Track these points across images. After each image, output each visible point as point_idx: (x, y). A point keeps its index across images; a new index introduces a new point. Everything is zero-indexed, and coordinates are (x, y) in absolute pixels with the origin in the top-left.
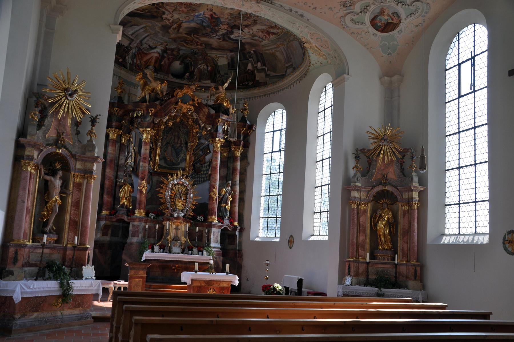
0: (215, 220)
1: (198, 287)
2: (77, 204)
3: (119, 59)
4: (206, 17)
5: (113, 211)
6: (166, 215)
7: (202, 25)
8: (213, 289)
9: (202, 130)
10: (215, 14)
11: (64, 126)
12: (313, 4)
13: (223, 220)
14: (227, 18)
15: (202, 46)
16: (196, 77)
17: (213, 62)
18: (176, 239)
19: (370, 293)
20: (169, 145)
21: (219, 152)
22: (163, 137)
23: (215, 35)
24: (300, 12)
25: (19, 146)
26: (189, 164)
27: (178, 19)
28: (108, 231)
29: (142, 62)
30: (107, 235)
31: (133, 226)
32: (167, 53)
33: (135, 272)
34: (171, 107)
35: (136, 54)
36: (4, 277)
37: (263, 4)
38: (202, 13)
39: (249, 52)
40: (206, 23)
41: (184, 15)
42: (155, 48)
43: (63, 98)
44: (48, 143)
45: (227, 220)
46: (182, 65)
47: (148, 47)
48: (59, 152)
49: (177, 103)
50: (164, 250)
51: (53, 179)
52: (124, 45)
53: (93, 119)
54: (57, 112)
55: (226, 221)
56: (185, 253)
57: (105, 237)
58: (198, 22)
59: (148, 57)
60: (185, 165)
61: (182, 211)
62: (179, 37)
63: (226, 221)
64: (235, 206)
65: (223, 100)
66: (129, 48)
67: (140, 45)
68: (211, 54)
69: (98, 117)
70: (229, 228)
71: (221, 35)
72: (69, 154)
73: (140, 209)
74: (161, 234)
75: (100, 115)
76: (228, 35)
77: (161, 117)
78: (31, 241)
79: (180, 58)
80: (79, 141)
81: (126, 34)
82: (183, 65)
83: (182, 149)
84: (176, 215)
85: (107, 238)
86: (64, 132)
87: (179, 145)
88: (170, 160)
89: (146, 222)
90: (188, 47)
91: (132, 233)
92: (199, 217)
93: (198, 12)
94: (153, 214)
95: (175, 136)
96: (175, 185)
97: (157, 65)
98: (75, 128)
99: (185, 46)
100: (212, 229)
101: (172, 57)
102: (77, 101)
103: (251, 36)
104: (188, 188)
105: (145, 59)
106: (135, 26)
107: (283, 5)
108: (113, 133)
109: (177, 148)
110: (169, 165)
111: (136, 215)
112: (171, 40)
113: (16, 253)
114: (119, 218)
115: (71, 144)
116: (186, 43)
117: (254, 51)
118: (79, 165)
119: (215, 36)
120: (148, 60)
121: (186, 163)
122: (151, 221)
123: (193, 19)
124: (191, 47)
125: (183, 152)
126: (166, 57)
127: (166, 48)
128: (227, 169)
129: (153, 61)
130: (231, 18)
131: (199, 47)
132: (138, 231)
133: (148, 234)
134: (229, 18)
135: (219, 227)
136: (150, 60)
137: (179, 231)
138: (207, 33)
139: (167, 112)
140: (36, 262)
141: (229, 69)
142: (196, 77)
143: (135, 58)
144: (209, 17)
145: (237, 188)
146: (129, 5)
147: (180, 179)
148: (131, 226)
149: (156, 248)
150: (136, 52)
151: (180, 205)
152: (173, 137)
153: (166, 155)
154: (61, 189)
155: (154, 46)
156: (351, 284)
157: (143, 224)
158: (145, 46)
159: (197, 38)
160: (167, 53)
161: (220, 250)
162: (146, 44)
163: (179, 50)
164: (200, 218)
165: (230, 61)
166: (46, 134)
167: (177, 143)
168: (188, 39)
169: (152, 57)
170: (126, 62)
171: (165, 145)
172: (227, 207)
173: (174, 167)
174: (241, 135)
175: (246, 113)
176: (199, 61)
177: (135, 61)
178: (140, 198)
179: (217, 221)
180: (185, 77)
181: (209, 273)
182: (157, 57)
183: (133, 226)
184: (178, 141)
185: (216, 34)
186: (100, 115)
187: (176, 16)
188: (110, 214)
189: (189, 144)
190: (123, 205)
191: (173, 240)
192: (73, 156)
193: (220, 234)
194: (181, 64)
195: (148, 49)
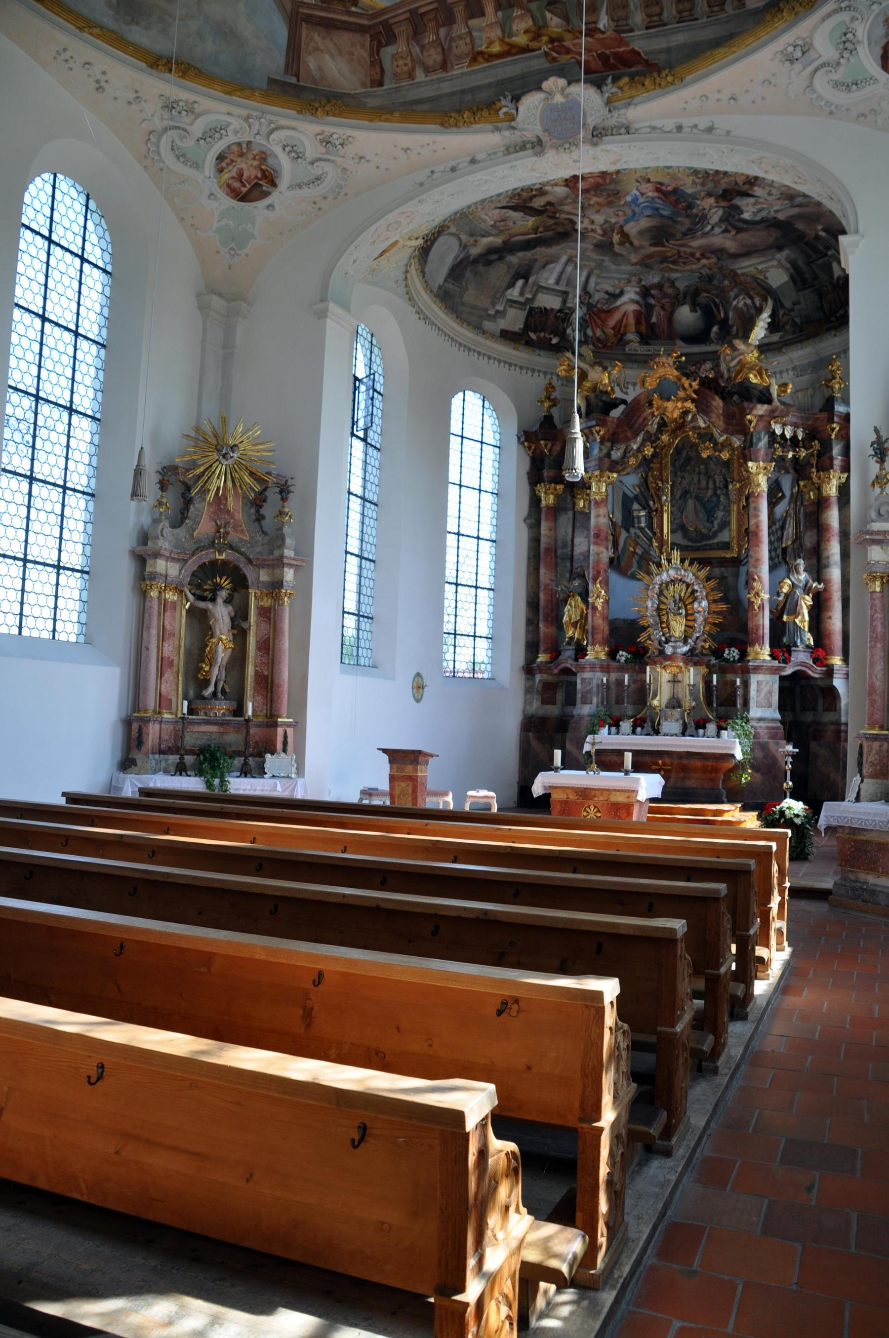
0: (763, 653)
1: (562, 802)
2: (268, 647)
3: (551, 339)
4: (653, 198)
5: (555, 653)
6: (650, 652)
7: (662, 216)
8: (595, 807)
9: (720, 451)
10: (661, 184)
12: (719, 91)
13: (790, 655)
14: (694, 182)
15: (708, 258)
16: (735, 329)
17: (758, 283)
18: (675, 703)
19: (882, 822)
20: (688, 496)
21: (765, 495)
22: (674, 482)
23: (709, 227)
24: (703, 123)
25: (141, 560)
26: (739, 531)
27: (606, 222)
28: (555, 694)
29: (605, 330)
30: (554, 703)
31: (583, 680)
32: (653, 297)
33: (398, 769)
34: (645, 414)
35: (587, 317)
37: (609, 143)
38: (635, 192)
39: (817, 237)
40: (664, 209)
41: (610, 211)
42: (622, 293)
45: (802, 653)
46: (696, 311)
47: (606, 297)
49: (651, 405)
50: (643, 728)
51: (210, 605)
52: (552, 309)
54: (205, 491)
55: (801, 658)
56: (687, 733)
57: (549, 707)
58: (649, 212)
59: (617, 316)
60: (730, 536)
61: (685, 642)
62: (651, 256)
63: (801, 658)
64: (830, 618)
65: (751, 369)
66: (567, 311)
67: (587, 298)
68: (743, 268)
69: (289, 483)
70: (810, 673)
71: (721, 220)
72: (242, 559)
73: (593, 644)
74: (642, 694)
76: (734, 217)
77: (627, 440)
79: (685, 298)
80: (263, 532)
81: (542, 284)
82: (699, 312)
83: (719, 501)
84: (669, 650)
85: (553, 710)
87: (710, 493)
88: (696, 528)
89: (606, 669)
90: (684, 271)
91: (582, 697)
92: (727, 652)
93: (627, 194)
94: (624, 653)
95: (699, 473)
96: (667, 584)
97: (643, 328)
98: (253, 511)
99: (676, 271)
100: (752, 676)
101: (667, 300)
103: (786, 199)
104: (696, 587)
105: (612, 322)
106: (552, 265)
107: (658, 123)
108: (546, 493)
109: (708, 501)
110: (690, 540)
111: (587, 658)
112: (638, 267)
114: (563, 666)
116: (673, 263)
117: (824, 230)
118: (264, 576)
119: (712, 228)
120: (618, 322)
121: (730, 530)
122: (622, 669)
123: (634, 214)
124: (688, 268)
125: (721, 507)
126: (655, 306)
127: (643, 286)
128: (818, 530)
129: (632, 320)
130: (702, 180)
131: (704, 261)
132: (590, 691)
133: (617, 697)
134: (698, 181)
135: (773, 671)
136: (624, 321)
137: (680, 684)
138: (690, 230)
139: (636, 426)
141: (799, 290)
142: (735, 329)
143: (587, 327)
144: (655, 194)
145: (835, 574)
147: (677, 569)
148: (579, 681)
149: (626, 725)
150: (585, 314)
151: (678, 627)
152: (696, 478)
153: (684, 520)
155: (617, 291)
156: (858, 799)
157: (599, 674)
158: (597, 297)
159: (683, 245)
160: (653, 297)
161: (779, 724)
162: (598, 291)
163: (672, 283)
164: (732, 653)
165: (792, 270)
167: (707, 488)
168: (669, 254)
169: (625, 313)
170: (570, 341)
171: (680, 498)
172: (797, 621)
173: (705, 543)
174: (834, 443)
175: (837, 386)
176: (728, 292)
177: (589, 332)
178: (593, 621)
179: (769, 658)
180: (713, 335)
181: (584, 773)
182: (634, 311)
183: (583, 680)
184: (708, 483)
185: (708, 223)
187: (599, 219)
188: (551, 662)
189: (730, 487)
190: (571, 638)
191: (667, 707)
192: (250, 561)
193: (777, 686)
194: (693, 310)
195: (607, 301)
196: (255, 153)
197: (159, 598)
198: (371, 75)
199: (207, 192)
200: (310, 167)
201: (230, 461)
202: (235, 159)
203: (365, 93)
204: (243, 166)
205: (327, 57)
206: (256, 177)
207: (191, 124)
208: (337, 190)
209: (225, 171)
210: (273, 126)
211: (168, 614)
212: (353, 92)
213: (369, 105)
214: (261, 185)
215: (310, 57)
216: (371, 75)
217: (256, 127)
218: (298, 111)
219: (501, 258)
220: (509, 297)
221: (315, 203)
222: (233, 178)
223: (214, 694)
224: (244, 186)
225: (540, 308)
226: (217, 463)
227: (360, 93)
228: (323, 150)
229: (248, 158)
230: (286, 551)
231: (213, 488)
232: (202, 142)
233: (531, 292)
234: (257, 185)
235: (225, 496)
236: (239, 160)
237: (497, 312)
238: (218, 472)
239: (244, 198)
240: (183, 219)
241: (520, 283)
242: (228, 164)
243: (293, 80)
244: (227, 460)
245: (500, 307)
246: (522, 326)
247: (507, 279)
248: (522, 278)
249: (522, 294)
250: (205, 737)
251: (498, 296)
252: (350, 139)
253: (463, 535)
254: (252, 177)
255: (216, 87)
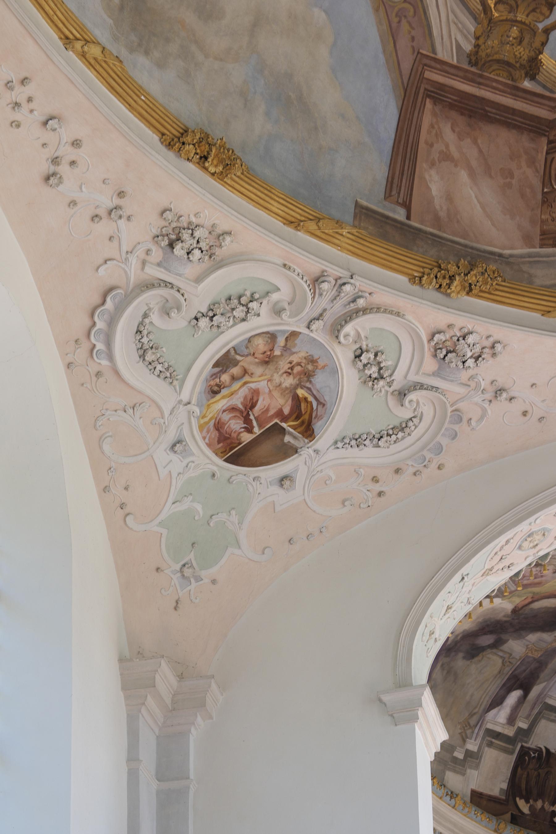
146: (443, 594)
196: (295, 359)
198: (542, 221)
199: (171, 436)
200: (392, 402)
202: (252, 368)
203: (530, 255)
204: (262, 385)
205: (464, 175)
206: (279, 414)
207: (199, 280)
208: (428, 456)
209: (224, 392)
210: (361, 303)
212: (507, 252)
213: (538, 282)
214: (283, 431)
215: (433, 172)
216: (542, 221)
217: (323, 302)
218: (412, 279)
219: (497, 644)
220: (490, 726)
221: (375, 480)
222: (233, 409)
224: (249, 430)
225: (539, 750)
227: (522, 256)
228: (430, 364)
229: (277, 370)
232: (204, 322)
233: (527, 717)
234: (277, 430)
236: (258, 370)
237: (469, 754)
239: (234, 460)
240: (106, 489)
241: (514, 696)
242: (234, 379)
243: (400, 214)
245: (472, 746)
246: (505, 786)
247: (494, 688)
248: (520, 687)
249: (511, 720)
251: (473, 722)
252: (498, 347)
254: (271, 412)
255: (275, 207)
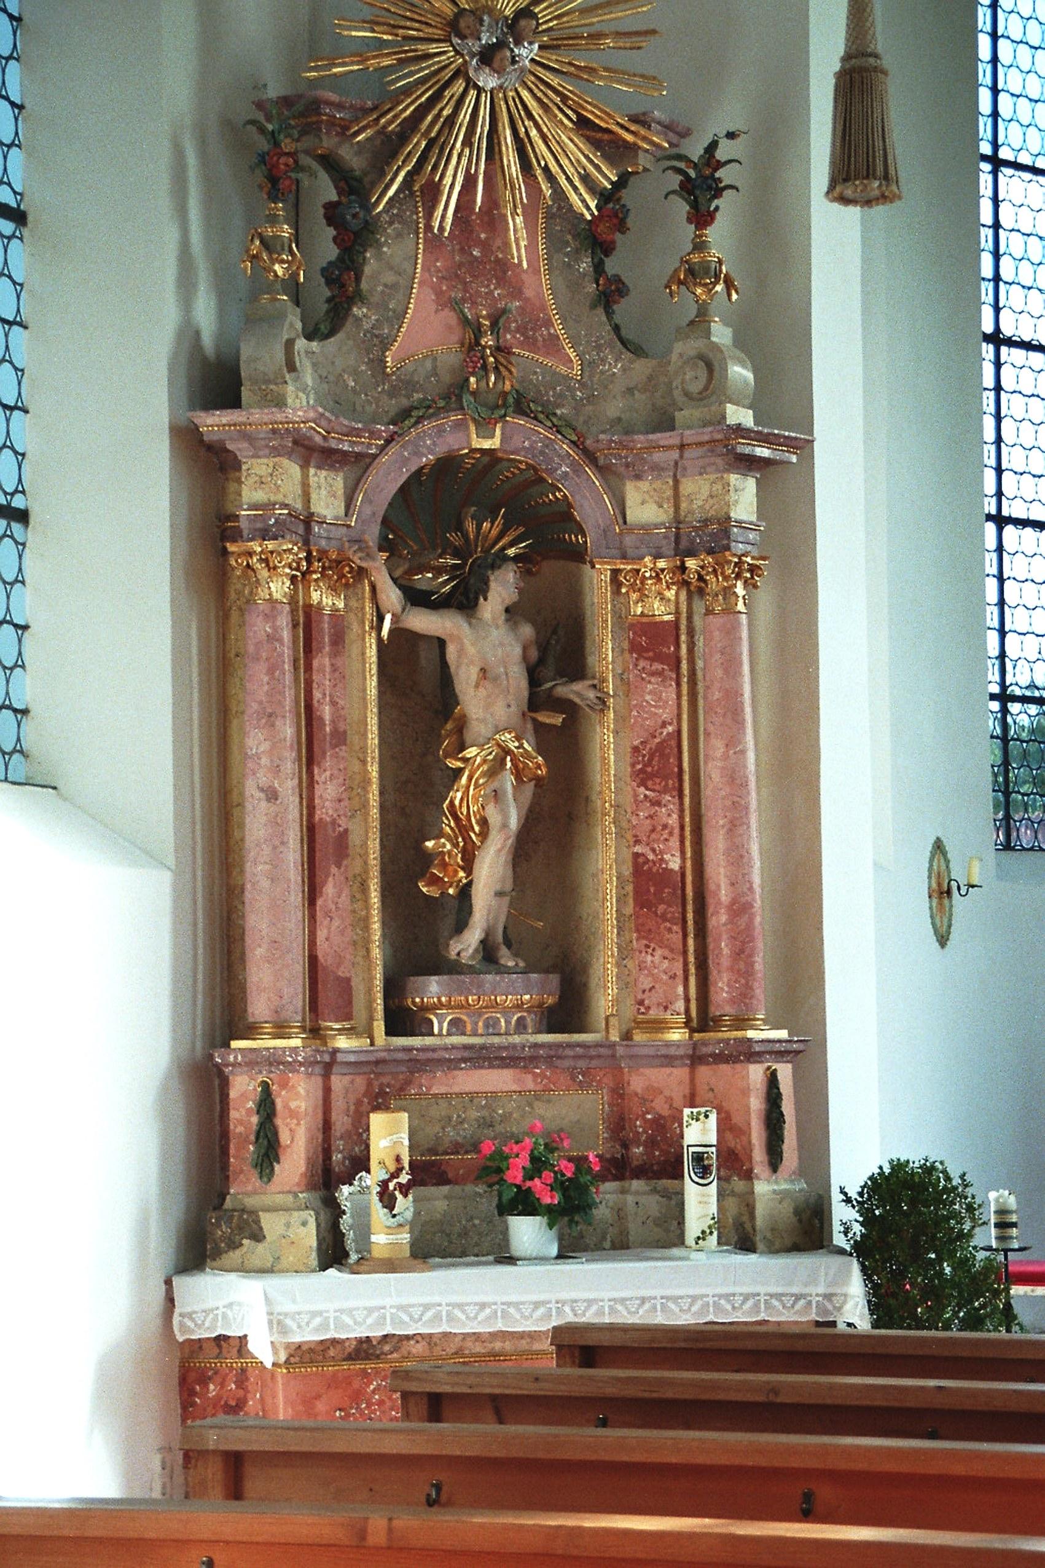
11: (502, 269)
36: (217, 1254)
43: (447, 94)
44: (405, 402)
48: (487, 444)
53: (692, 174)
69: (721, 155)
75: (731, 135)
78: (379, 1027)
80: (623, 342)
86: (504, 311)
98: (585, 265)
102: (554, 81)
113: (266, 1105)
115: (567, 378)
140: (433, 1151)
154: (534, 680)
166: (385, 344)
186: (731, 135)
197: (293, 600)
201: (511, 80)
211: (322, 661)
223: (488, 952)
226: (459, 86)
230: (730, 408)
231: (452, 181)
235: (493, 217)
238: (464, 117)
244: (499, 72)
250: (474, 1114)
253: (1010, 343)
